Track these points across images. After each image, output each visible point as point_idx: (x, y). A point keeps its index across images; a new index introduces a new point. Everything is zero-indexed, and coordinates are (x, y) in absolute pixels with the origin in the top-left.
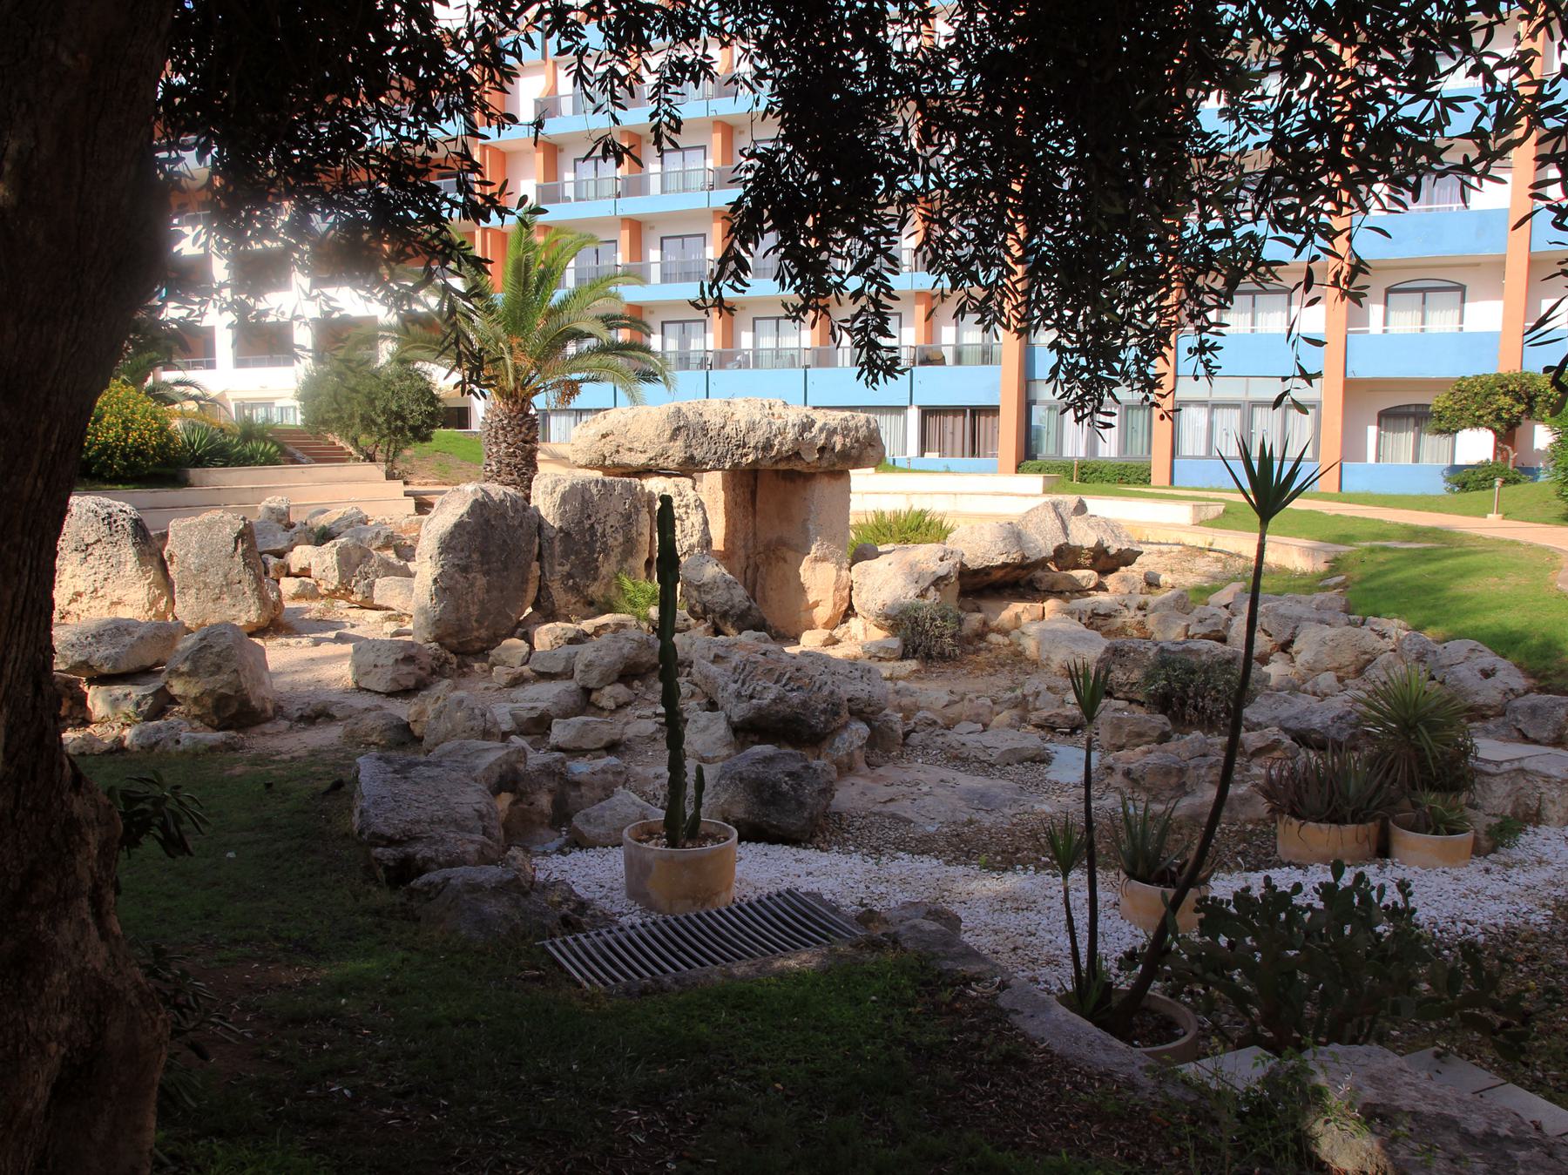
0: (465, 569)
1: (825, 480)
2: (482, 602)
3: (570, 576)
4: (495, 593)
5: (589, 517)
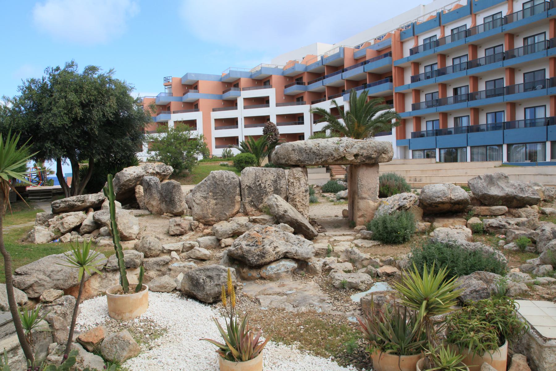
0: (205, 198)
1: (365, 168)
2: (213, 209)
3: (252, 201)
4: (219, 206)
5: (258, 181)
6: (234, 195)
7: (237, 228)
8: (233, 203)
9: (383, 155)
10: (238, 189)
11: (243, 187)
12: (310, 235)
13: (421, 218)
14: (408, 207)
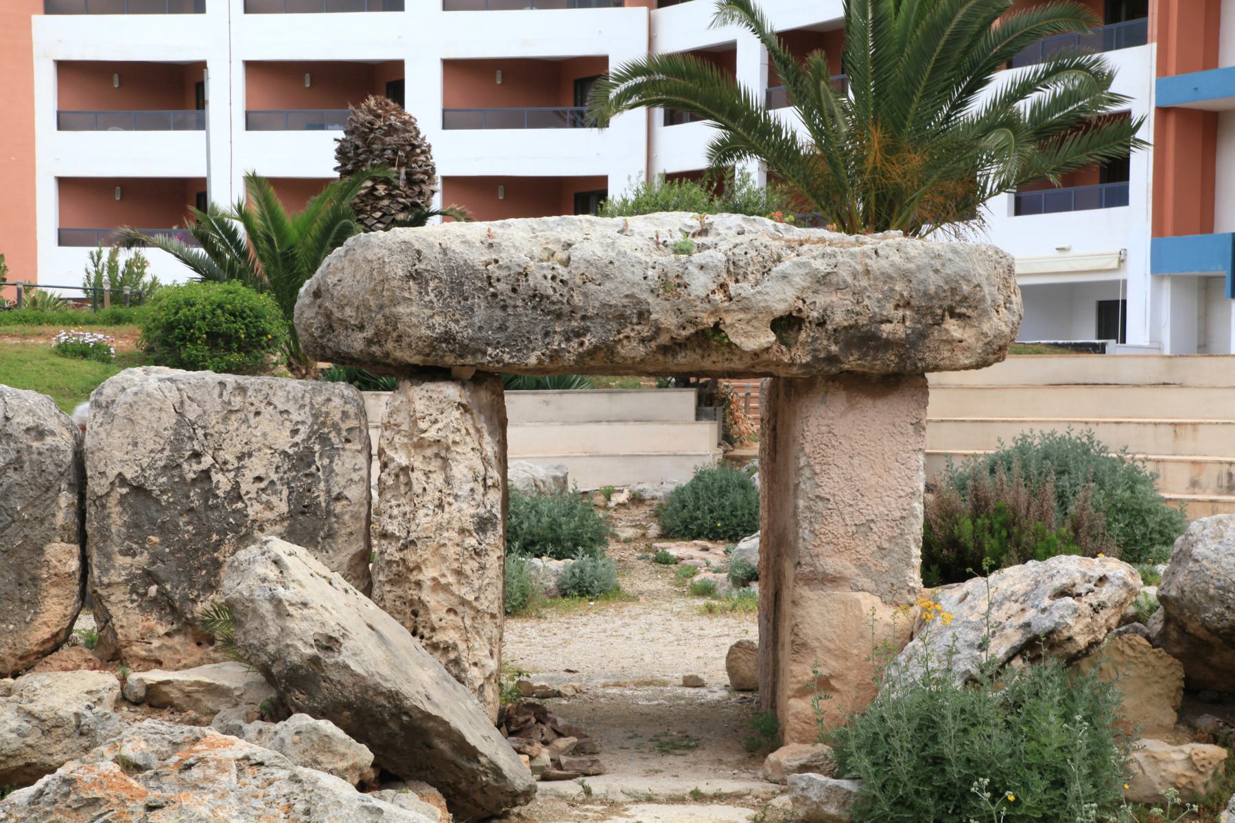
3: (150, 576)
5: (197, 455)
6: (37, 533)
7: (15, 743)
8: (28, 584)
9: (953, 328)
10: (66, 499)
11: (96, 486)
12: (484, 788)
13: (1170, 717)
14: (1082, 641)
